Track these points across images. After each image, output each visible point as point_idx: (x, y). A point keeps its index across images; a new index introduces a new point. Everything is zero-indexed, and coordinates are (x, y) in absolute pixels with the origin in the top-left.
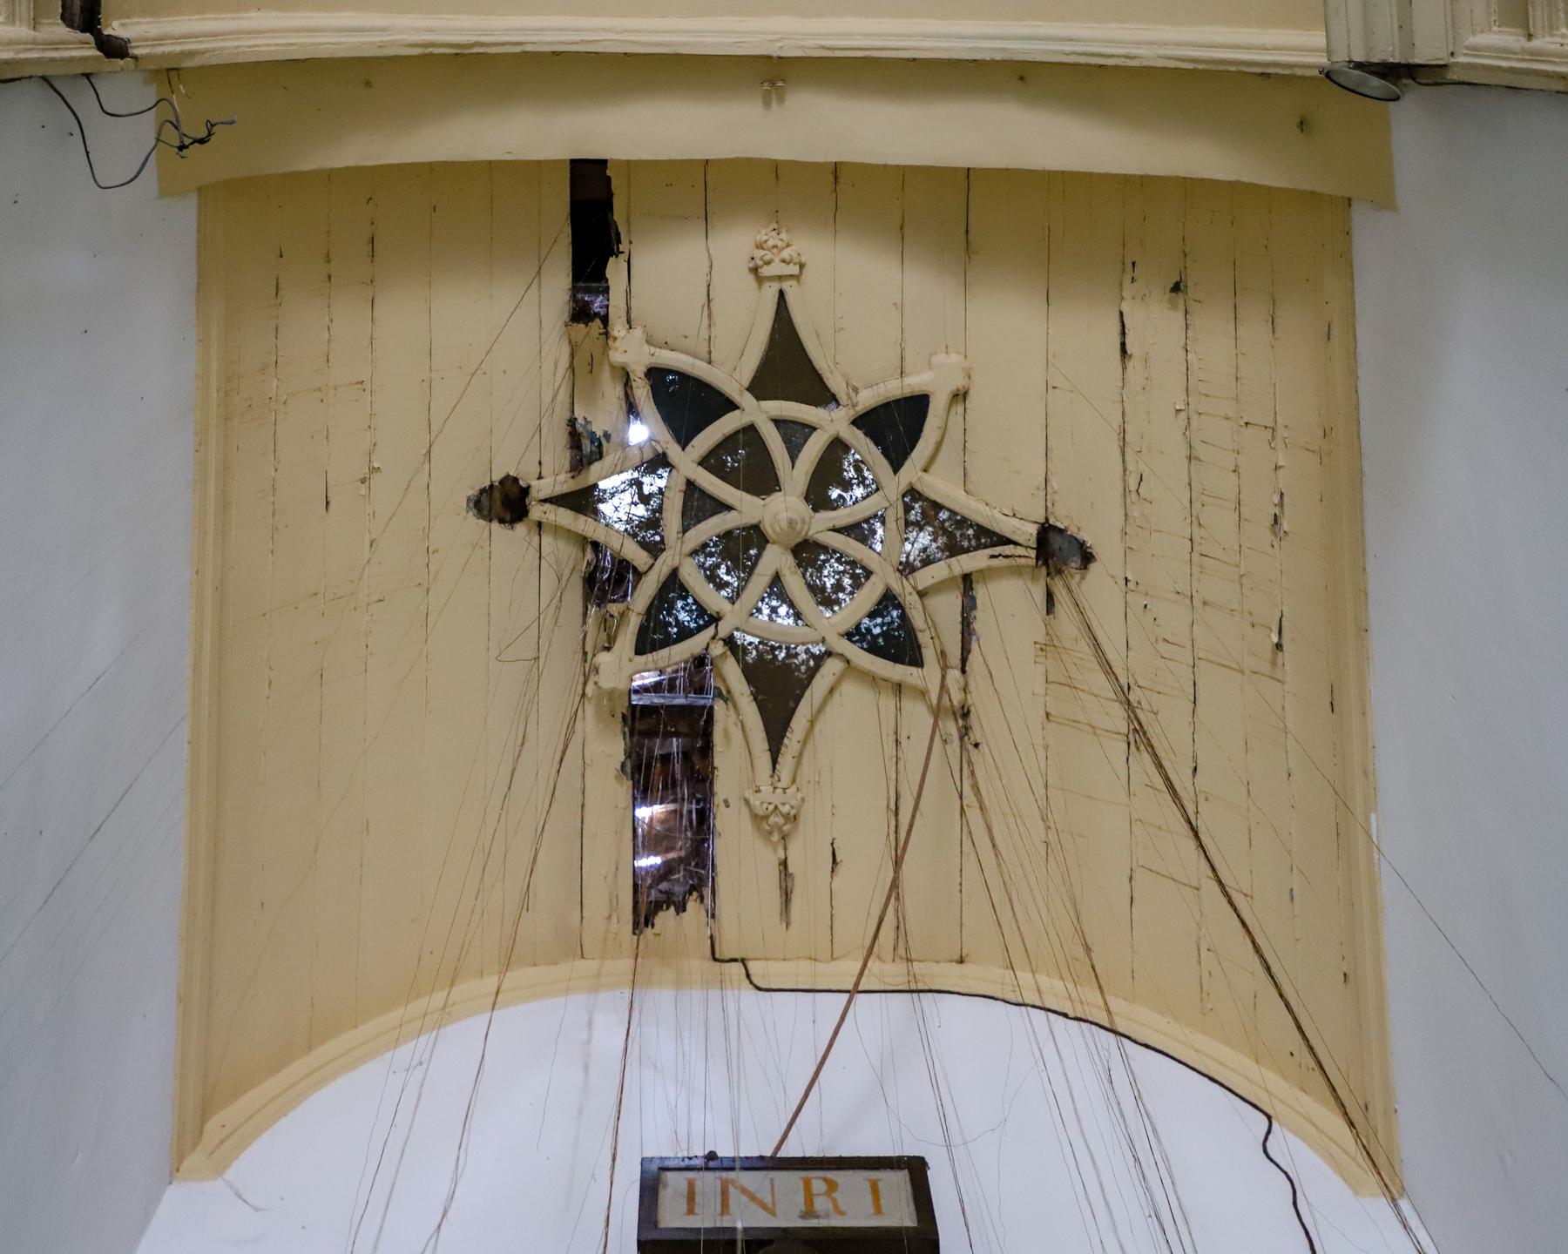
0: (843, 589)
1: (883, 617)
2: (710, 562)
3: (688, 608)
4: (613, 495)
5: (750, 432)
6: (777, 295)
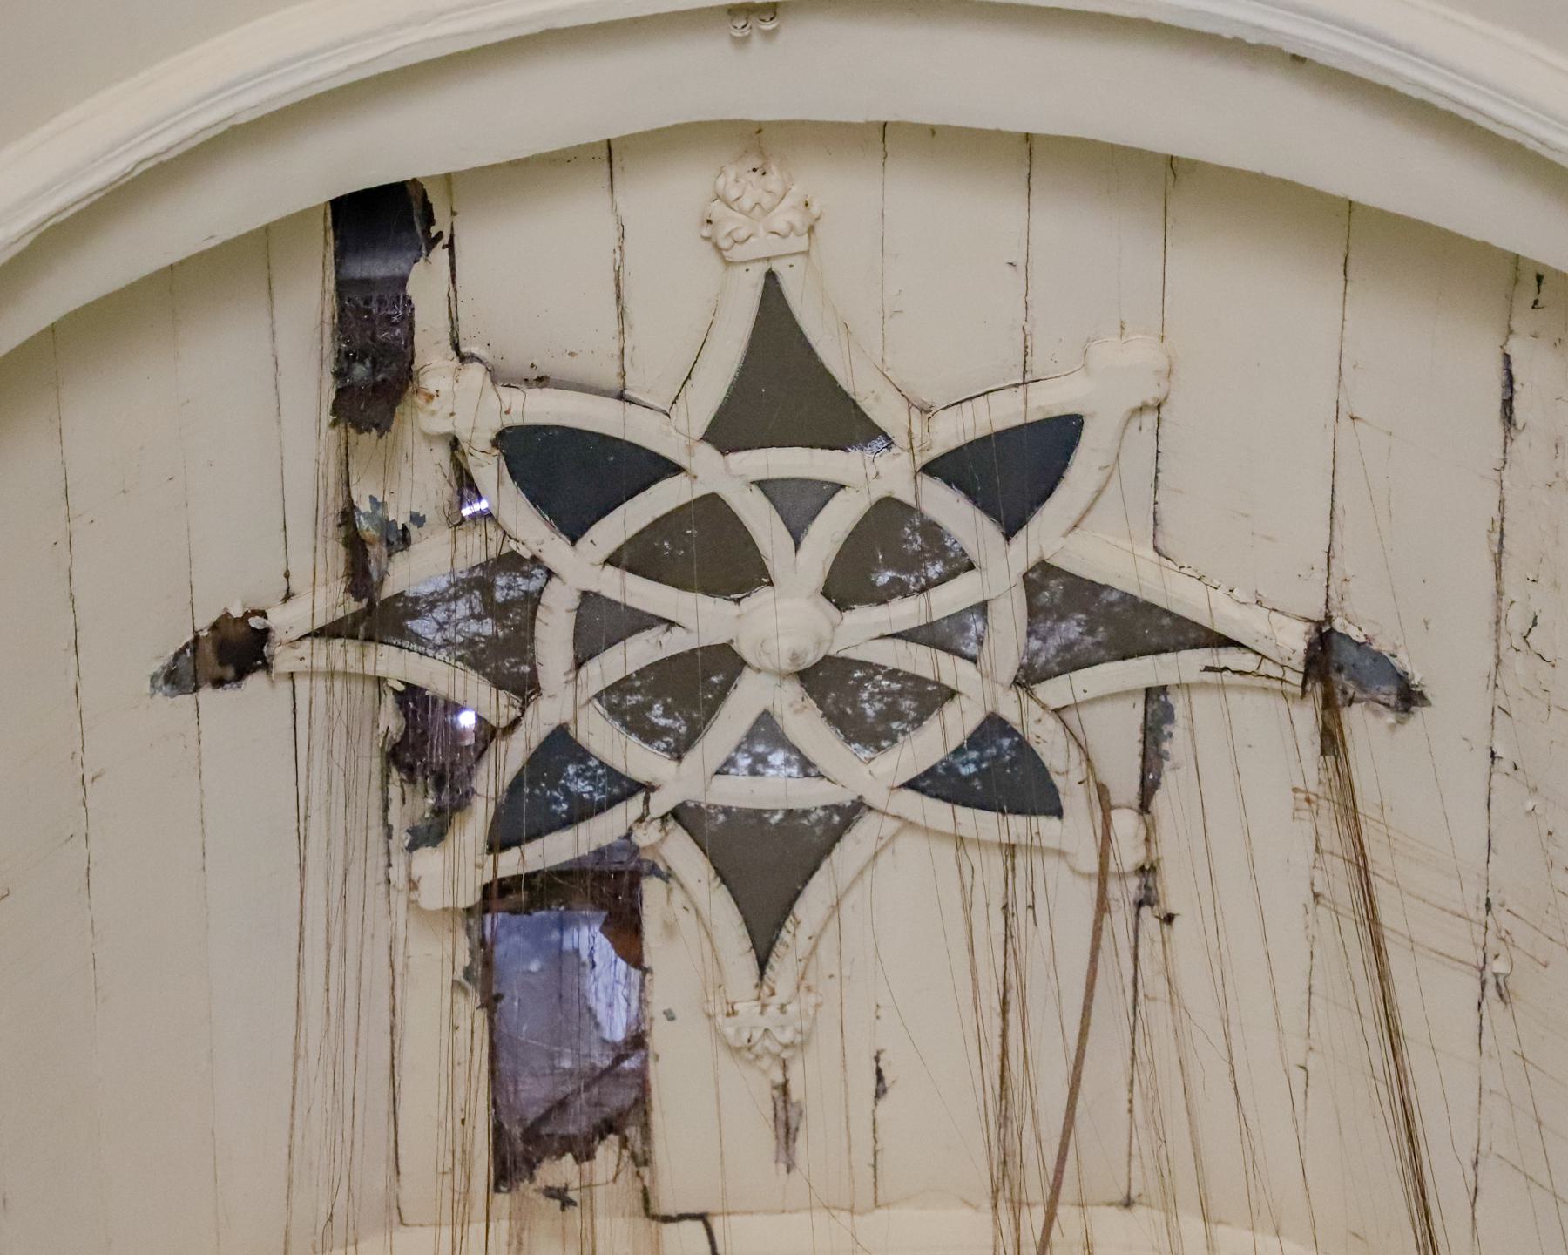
0: (901, 717)
1: (981, 750)
2: (632, 700)
3: (589, 774)
4: (433, 605)
5: (712, 507)
6: (762, 281)
